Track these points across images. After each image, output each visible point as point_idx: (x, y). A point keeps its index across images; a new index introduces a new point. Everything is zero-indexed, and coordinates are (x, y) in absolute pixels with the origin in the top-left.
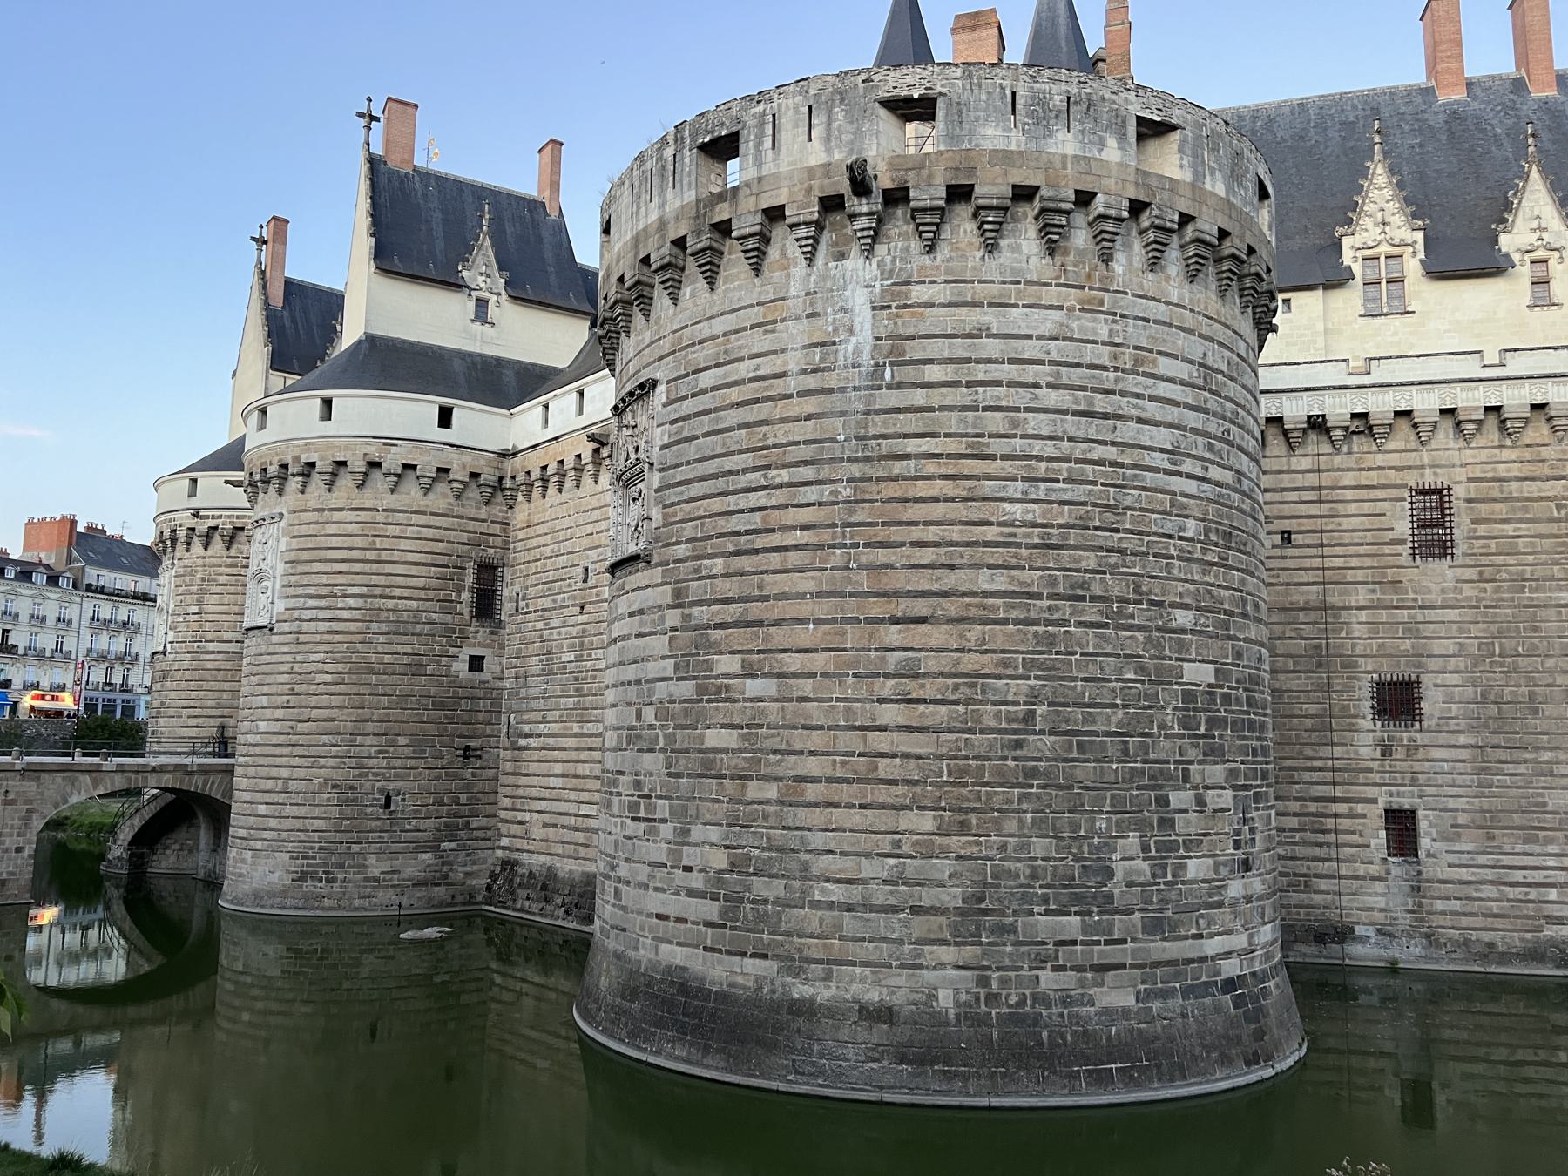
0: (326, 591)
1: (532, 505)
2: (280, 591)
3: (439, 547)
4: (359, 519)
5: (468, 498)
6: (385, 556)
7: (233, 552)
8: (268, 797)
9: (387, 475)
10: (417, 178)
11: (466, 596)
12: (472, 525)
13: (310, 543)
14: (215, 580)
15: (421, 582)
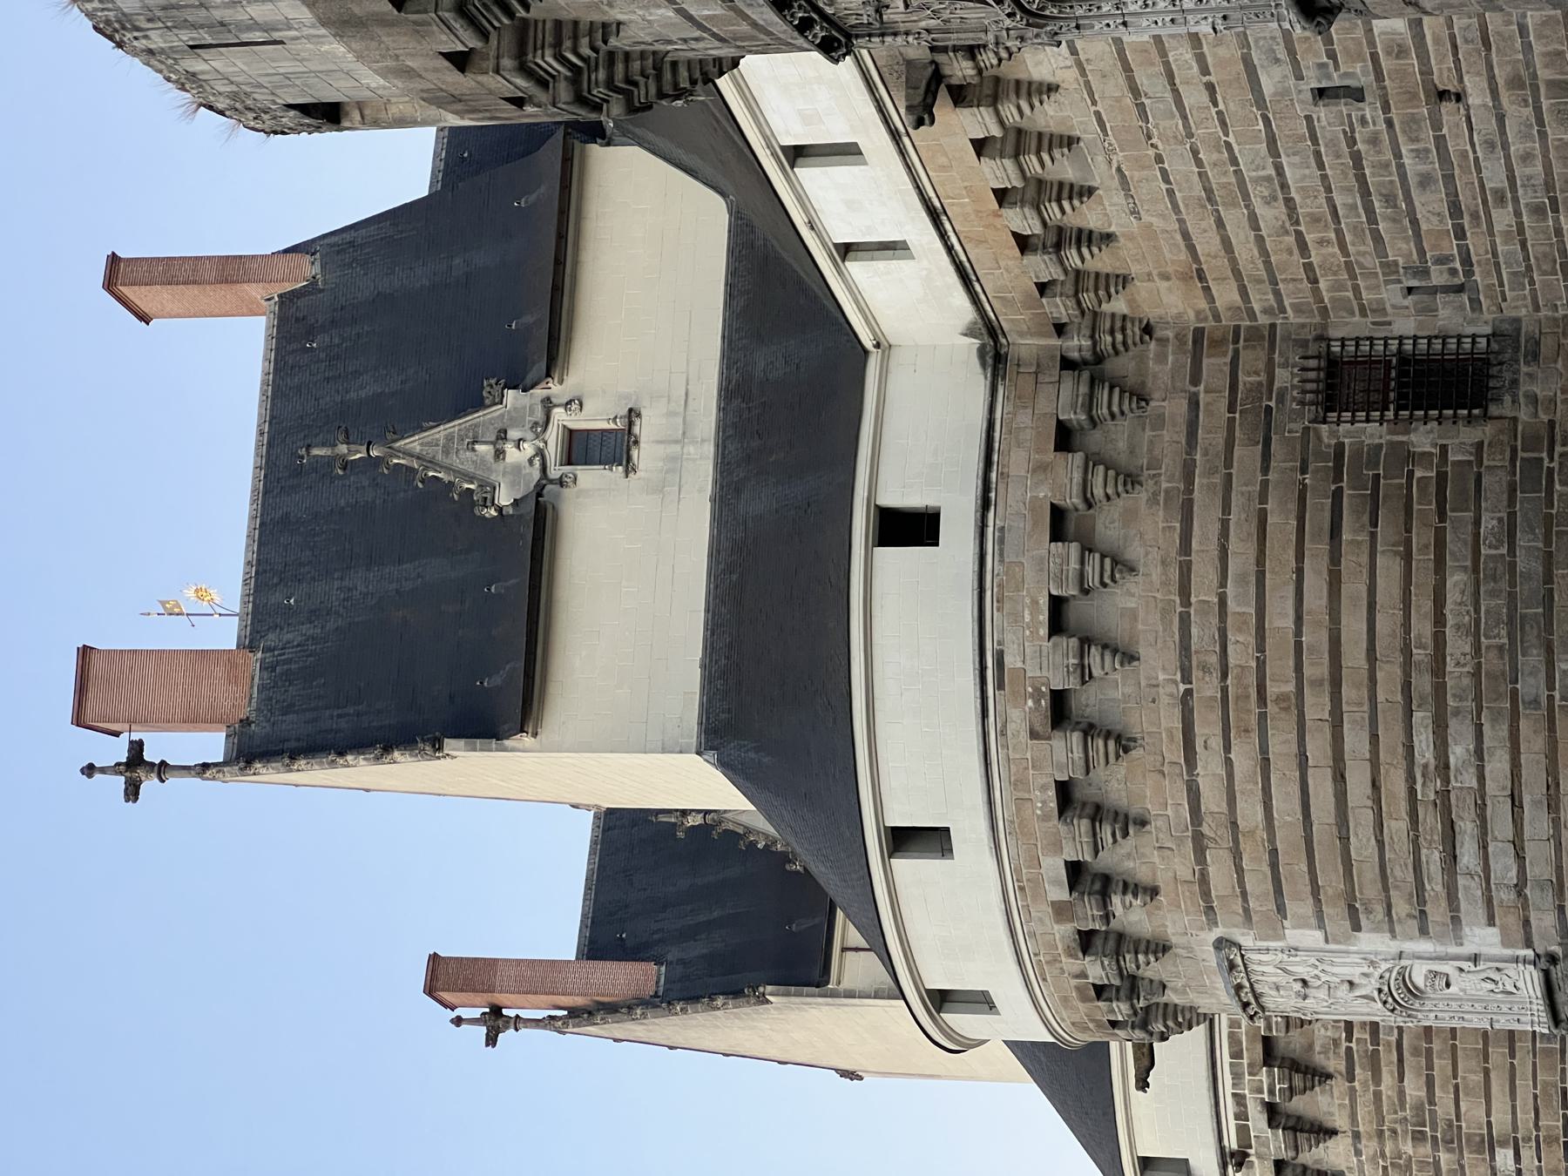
0: (1430, 821)
1: (1135, 269)
2: (1440, 939)
3: (1281, 522)
4: (1216, 743)
5: (1132, 451)
6: (1316, 668)
7: (1335, 1064)
9: (1085, 675)
10: (272, 638)
11: (1423, 438)
12: (1211, 436)
13: (1294, 867)
14: (1419, 1108)
15: (1389, 569)
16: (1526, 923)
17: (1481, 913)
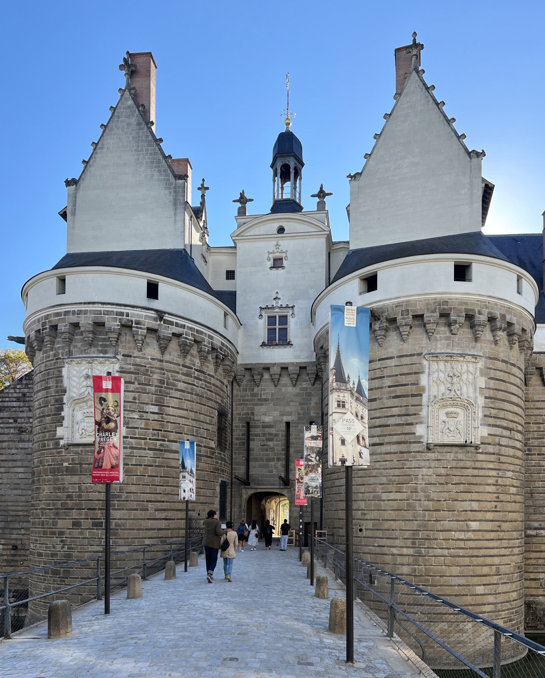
8: (485, 580)
13: (503, 386)
14: (174, 385)
16: (489, 444)
17: (492, 433)
